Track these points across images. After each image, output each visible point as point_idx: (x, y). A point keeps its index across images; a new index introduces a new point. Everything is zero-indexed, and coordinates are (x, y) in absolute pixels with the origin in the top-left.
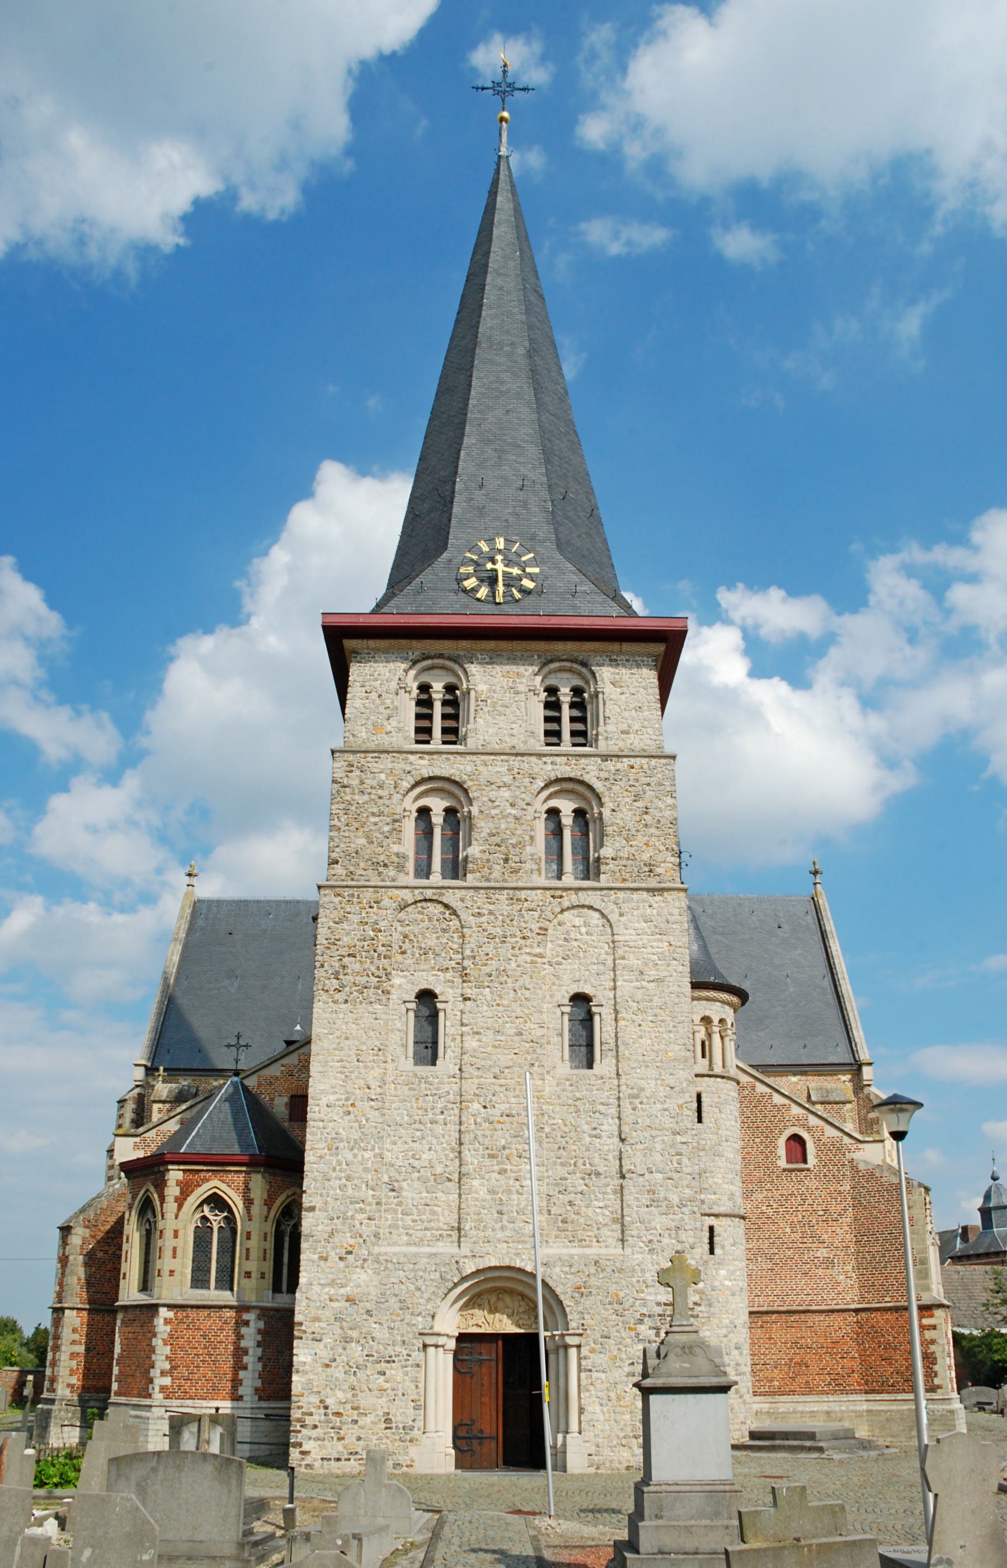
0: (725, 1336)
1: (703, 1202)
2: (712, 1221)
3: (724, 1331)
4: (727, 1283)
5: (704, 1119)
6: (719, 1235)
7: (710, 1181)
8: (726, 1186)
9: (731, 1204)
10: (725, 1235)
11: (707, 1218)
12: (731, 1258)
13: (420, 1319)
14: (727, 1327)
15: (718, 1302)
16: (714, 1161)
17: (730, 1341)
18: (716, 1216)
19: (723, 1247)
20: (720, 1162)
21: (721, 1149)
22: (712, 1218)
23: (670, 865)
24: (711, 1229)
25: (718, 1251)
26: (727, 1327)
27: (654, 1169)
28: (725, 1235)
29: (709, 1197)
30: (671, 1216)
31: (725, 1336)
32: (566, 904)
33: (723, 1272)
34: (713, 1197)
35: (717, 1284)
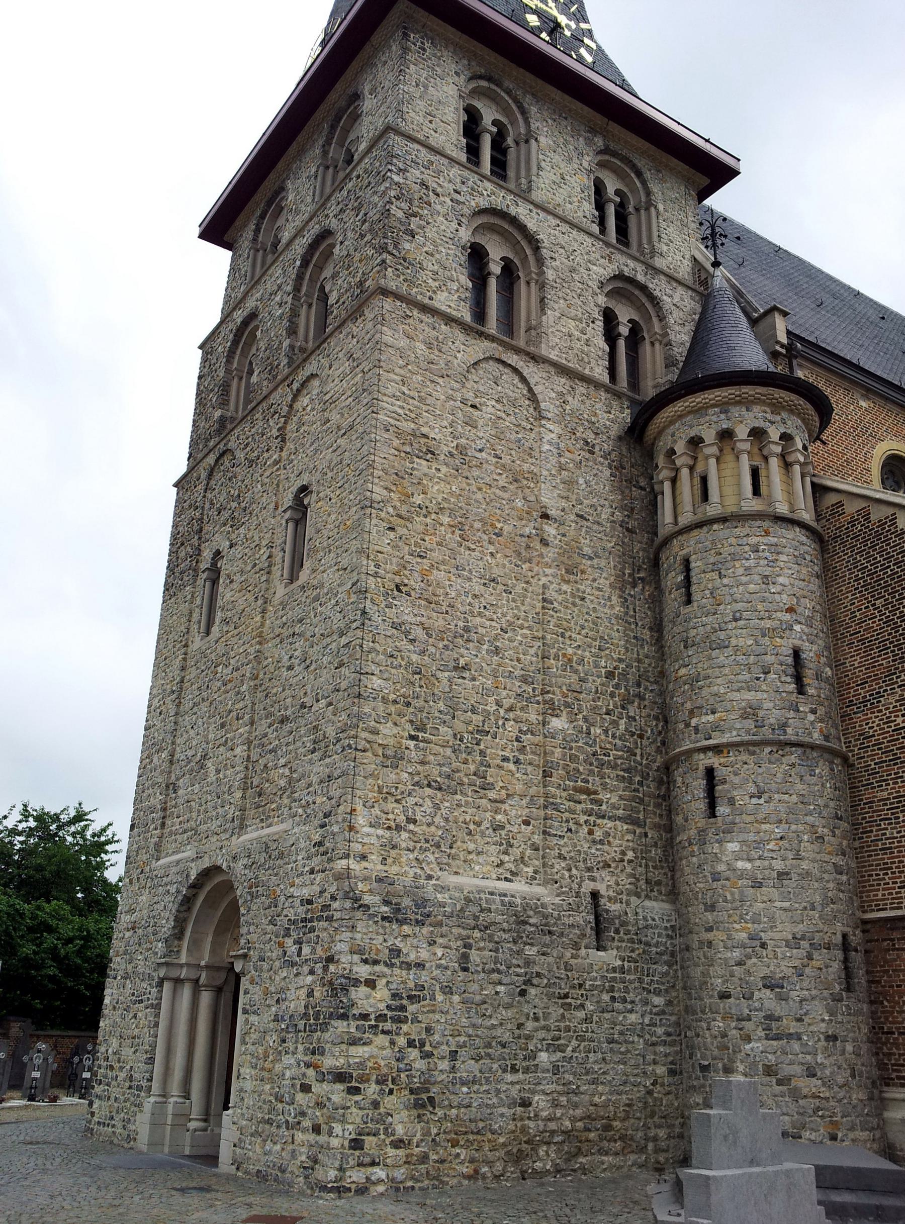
0: (740, 963)
1: (696, 729)
2: (713, 760)
3: (737, 954)
4: (740, 864)
5: (696, 596)
6: (724, 782)
7: (705, 692)
8: (736, 696)
9: (750, 724)
10: (736, 780)
11: (702, 756)
12: (749, 819)
13: (160, 944)
14: (744, 946)
15: (726, 901)
16: (710, 658)
17: (749, 973)
18: (717, 749)
19: (731, 802)
20: (721, 657)
21: (722, 635)
22: (710, 754)
23: (378, 268)
24: (710, 773)
25: (722, 810)
26: (744, 946)
27: (320, 696)
28: (736, 780)
29: (704, 719)
30: (327, 760)
31: (740, 963)
32: (295, 386)
33: (733, 847)
34: (711, 718)
35: (721, 868)
